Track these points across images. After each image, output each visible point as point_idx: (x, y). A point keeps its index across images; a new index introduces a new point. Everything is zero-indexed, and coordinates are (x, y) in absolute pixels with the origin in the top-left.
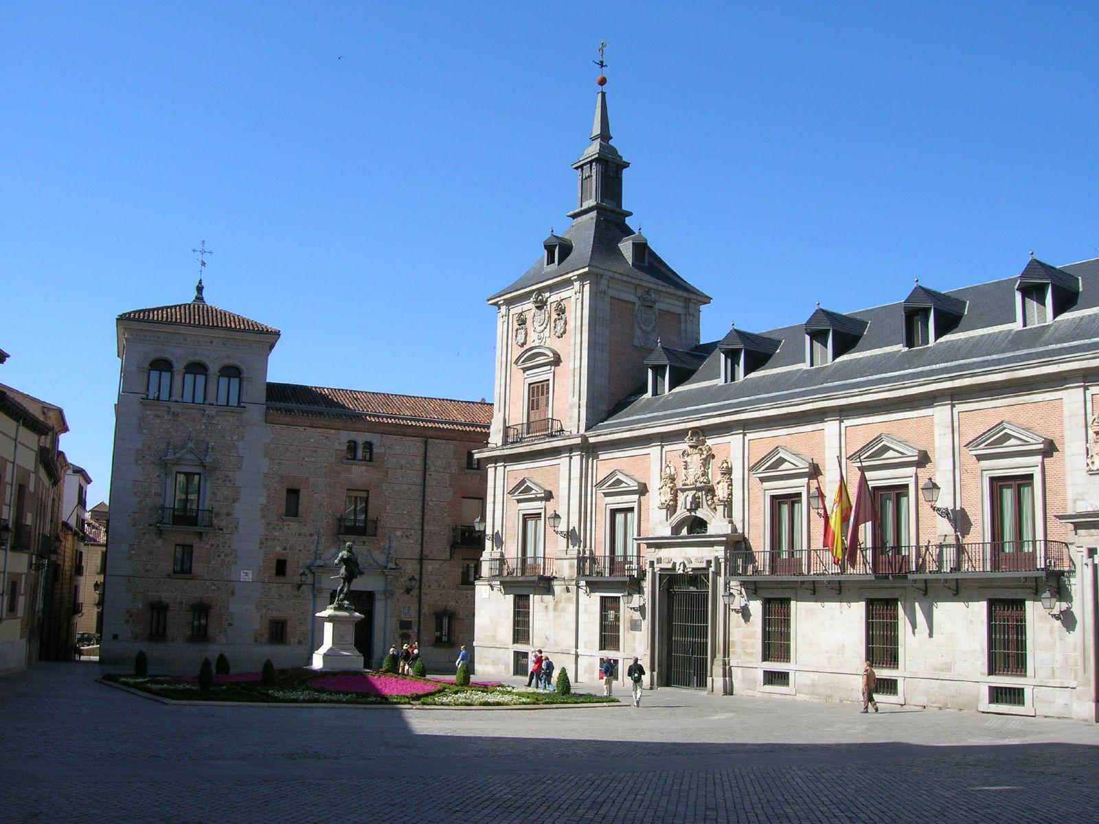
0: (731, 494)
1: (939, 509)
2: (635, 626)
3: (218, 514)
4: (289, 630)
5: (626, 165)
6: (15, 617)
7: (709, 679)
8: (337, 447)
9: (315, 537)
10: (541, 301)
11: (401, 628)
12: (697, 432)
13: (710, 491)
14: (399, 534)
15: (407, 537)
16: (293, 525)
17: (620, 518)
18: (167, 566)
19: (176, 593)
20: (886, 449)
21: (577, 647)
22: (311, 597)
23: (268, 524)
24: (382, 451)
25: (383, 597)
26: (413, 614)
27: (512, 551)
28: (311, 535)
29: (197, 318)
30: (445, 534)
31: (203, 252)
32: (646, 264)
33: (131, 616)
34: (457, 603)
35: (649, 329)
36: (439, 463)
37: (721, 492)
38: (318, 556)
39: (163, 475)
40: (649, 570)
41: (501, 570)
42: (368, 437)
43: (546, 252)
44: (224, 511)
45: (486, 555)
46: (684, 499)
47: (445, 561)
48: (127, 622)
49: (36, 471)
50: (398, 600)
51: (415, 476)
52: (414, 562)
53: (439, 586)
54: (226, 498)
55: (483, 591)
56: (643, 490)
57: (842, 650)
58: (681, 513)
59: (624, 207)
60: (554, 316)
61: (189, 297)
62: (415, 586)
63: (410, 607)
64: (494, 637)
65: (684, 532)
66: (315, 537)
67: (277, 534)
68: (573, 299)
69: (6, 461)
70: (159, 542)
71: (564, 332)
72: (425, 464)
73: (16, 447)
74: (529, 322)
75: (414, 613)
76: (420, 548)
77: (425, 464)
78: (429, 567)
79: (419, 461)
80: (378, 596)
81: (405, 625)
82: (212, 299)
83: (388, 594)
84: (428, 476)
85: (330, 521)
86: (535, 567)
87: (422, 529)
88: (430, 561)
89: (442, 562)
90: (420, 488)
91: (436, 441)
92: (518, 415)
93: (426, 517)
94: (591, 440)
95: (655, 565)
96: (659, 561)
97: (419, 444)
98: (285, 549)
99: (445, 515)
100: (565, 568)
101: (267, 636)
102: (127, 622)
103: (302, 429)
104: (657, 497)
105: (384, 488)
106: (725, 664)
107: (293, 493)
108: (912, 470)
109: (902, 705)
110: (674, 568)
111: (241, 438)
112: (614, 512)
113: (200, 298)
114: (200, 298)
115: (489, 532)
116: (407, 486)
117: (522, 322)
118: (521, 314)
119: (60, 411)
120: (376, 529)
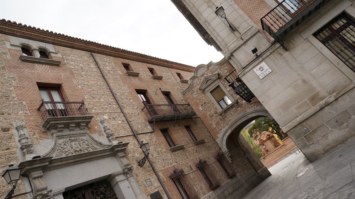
25: (122, 177)
30: (139, 114)
34: (177, 163)
38: (26, 148)
50: (137, 176)
55: (259, 73)
63: (149, 179)
64: (314, 99)
66: (14, 131)
75: (157, 184)
76: (128, 126)
79: (93, 66)
83: (127, 171)
85: (28, 112)
88: (141, 135)
89: (149, 134)
90: (104, 83)
91: (99, 55)
99: (131, 101)
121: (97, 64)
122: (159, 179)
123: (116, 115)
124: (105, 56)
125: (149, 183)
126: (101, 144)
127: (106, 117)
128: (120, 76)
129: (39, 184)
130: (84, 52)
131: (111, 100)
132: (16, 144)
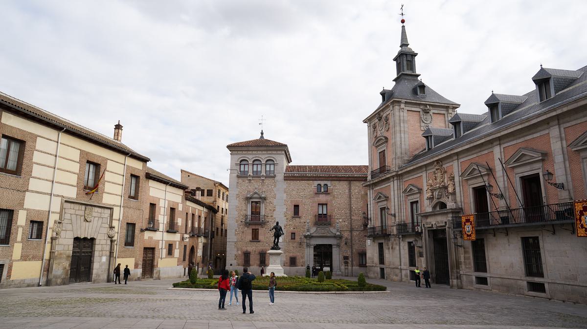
0: (455, 189)
1: (556, 184)
2: (421, 255)
3: (268, 216)
4: (298, 261)
5: (416, 55)
6: (174, 257)
7: (451, 280)
8: (313, 187)
9: (306, 223)
10: (380, 117)
12: (437, 161)
13: (446, 188)
14: (340, 222)
15: (344, 221)
16: (297, 219)
17: (415, 205)
18: (250, 237)
19: (253, 248)
20: (523, 155)
21: (401, 265)
22: (305, 247)
23: (287, 219)
24: (332, 187)
26: (349, 253)
27: (378, 224)
28: (305, 223)
29: (263, 145)
31: (262, 120)
35: (428, 122)
36: (356, 191)
37: (450, 190)
38: (308, 231)
39: (246, 203)
40: (423, 228)
41: (374, 232)
42: (326, 182)
43: (381, 97)
44: (269, 215)
45: (368, 226)
46: (436, 193)
47: (361, 231)
48: (235, 259)
49: (182, 203)
51: (346, 196)
53: (359, 241)
54: (270, 210)
56: (420, 191)
57: (512, 266)
58: (435, 201)
59: (417, 72)
60: (385, 123)
61: (258, 137)
62: (349, 243)
64: (373, 261)
65: (438, 209)
67: (291, 223)
68: (391, 114)
70: (246, 228)
71: (389, 128)
72: (350, 191)
74: (377, 127)
77: (350, 191)
78: (355, 233)
79: (347, 191)
80: (333, 246)
81: (346, 258)
82: (266, 137)
83: (338, 246)
86: (386, 230)
91: (354, 182)
92: (377, 166)
93: (352, 214)
94: (400, 173)
95: (425, 226)
96: (427, 223)
97: (347, 184)
98: (294, 229)
100: (395, 231)
101: (289, 263)
103: (299, 181)
104: (427, 195)
106: (457, 273)
107: (296, 207)
108: (539, 165)
109: (550, 299)
110: (432, 227)
111: (275, 186)
112: (412, 203)
113: (262, 137)
114: (262, 137)
115: (369, 217)
117: (375, 127)
118: (374, 124)
119: (221, 184)
120: (330, 220)
121: (350, 189)
122: (352, 252)
124: (358, 182)
125: (346, 252)
126: (332, 232)
127: (341, 220)
128: (361, 195)
129: (308, 242)
130: (346, 182)
131: (348, 212)
132: (306, 227)
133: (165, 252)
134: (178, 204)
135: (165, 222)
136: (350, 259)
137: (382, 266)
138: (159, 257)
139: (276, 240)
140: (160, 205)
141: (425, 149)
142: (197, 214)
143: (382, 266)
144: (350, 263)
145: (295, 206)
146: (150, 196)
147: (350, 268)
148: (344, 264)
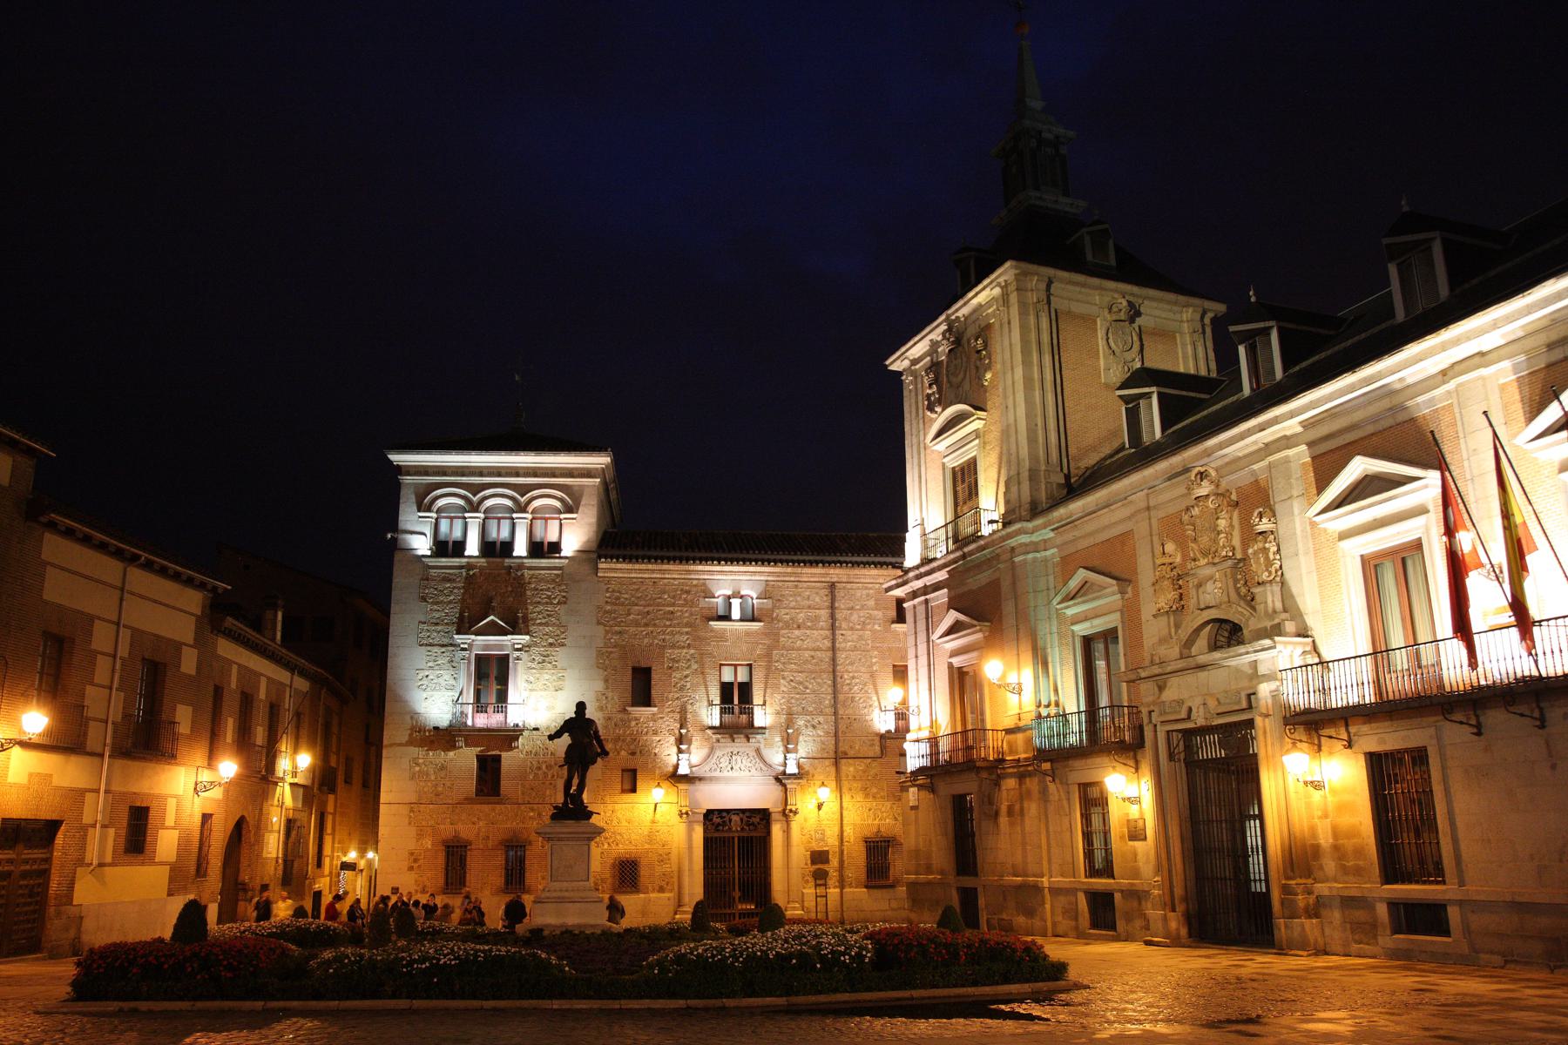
4: (644, 872)
11: (813, 863)
17: (1099, 647)
18: (471, 786)
32: (1113, 262)
33: (415, 861)
48: (411, 868)
49: (199, 642)
52: (827, 762)
69: (91, 619)
73: (121, 600)
84: (839, 638)
87: (835, 714)
90: (829, 654)
102: (411, 868)
105: (775, 658)
112: (1088, 642)
116: (807, 654)
121: (832, 607)
123: (821, 719)
133: (103, 842)
134: (178, 646)
135: (116, 714)
136: (834, 862)
137: (968, 882)
138: (81, 862)
139: (575, 781)
140: (94, 646)
141: (1122, 448)
142: (262, 695)
143: (968, 882)
144: (833, 874)
145: (636, 670)
146: (47, 603)
147: (833, 892)
148: (811, 879)
